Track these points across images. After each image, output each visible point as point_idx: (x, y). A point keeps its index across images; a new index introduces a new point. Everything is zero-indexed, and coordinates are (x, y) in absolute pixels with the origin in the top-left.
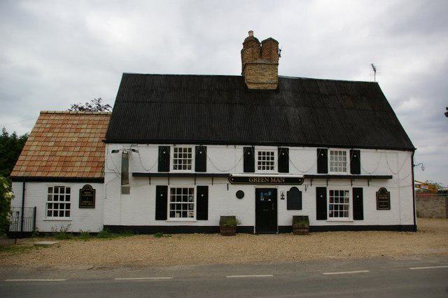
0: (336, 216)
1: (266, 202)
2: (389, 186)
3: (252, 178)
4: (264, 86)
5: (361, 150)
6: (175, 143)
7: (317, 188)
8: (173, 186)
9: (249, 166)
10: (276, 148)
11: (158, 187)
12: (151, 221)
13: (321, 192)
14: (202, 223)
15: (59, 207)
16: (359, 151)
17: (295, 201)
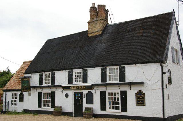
0: (113, 109)
1: (78, 100)
2: (144, 89)
3: (71, 87)
4: (95, 33)
5: (126, 66)
6: (44, 72)
7: (101, 91)
8: (45, 92)
9: (70, 81)
10: (82, 70)
11: (101, 92)
12: (35, 108)
13: (103, 94)
14: (124, 114)
15: (14, 103)
16: (87, 70)
17: (90, 100)
